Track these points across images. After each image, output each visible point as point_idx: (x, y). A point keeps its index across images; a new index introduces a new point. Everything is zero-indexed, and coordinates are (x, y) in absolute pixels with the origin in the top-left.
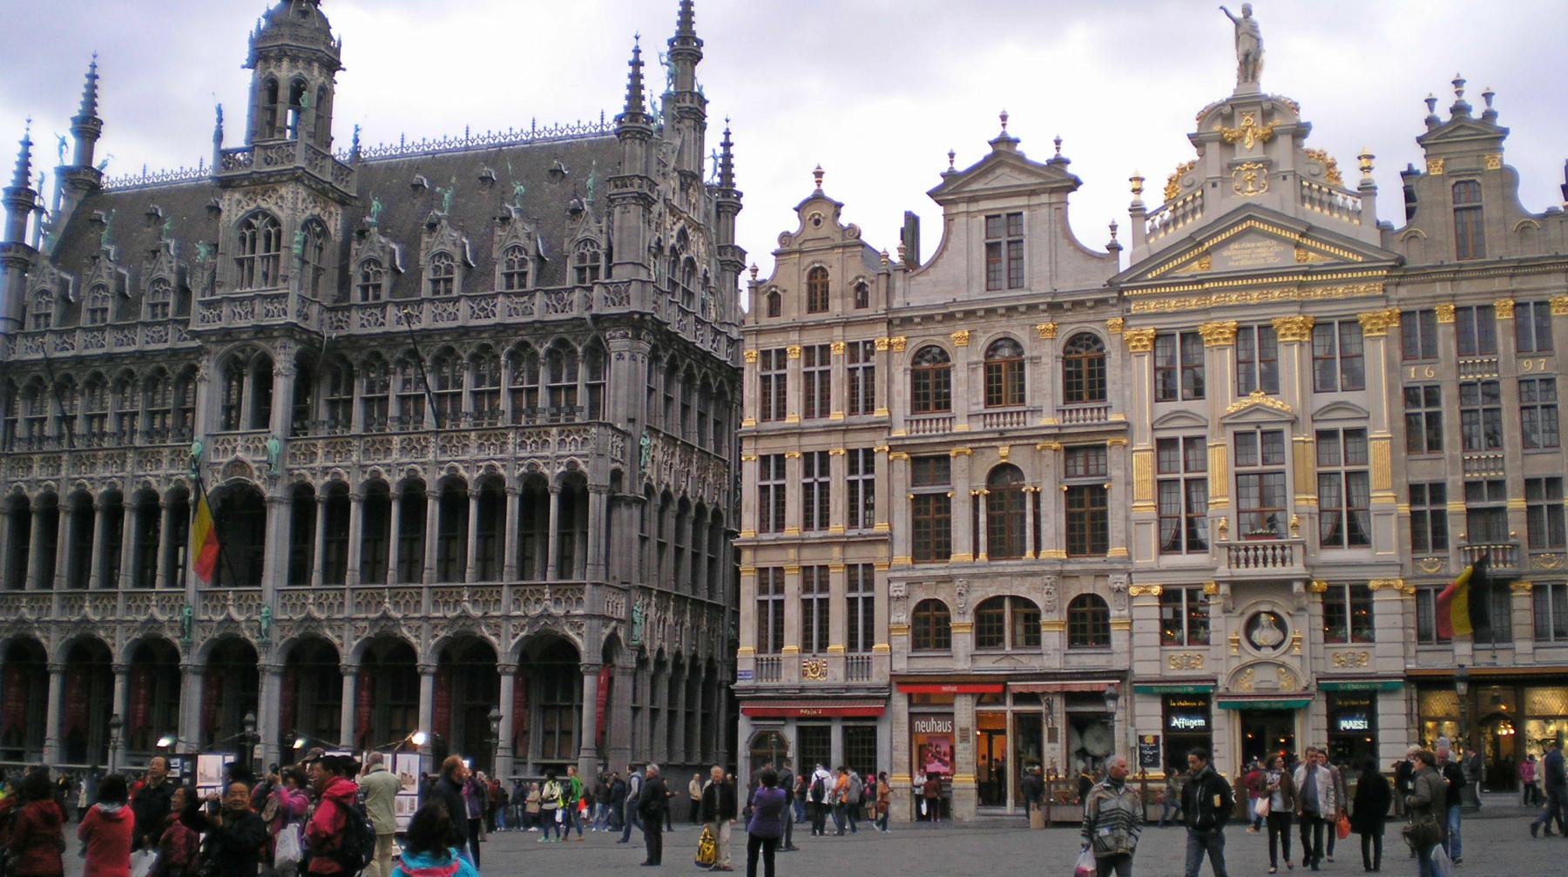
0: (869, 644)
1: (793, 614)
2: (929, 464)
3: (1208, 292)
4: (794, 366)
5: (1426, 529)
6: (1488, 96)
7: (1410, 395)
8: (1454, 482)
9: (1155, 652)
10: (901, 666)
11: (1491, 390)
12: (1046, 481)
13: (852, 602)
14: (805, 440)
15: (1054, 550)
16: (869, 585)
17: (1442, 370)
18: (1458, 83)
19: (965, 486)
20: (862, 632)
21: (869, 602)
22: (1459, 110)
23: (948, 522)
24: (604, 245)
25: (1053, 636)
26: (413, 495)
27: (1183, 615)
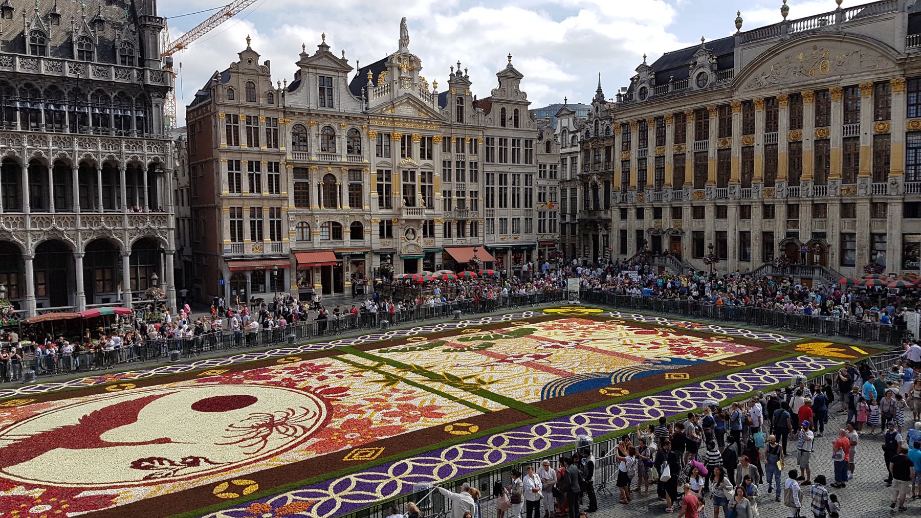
0: (280, 239)
1: (247, 227)
2: (301, 171)
3: (394, 121)
4: (242, 123)
5: (447, 204)
6: (466, 70)
7: (444, 162)
8: (454, 191)
9: (379, 241)
10: (294, 246)
11: (463, 163)
12: (344, 183)
13: (272, 223)
14: (249, 156)
15: (346, 206)
16: (279, 216)
17: (453, 156)
18: (459, 64)
19: (315, 180)
20: (277, 233)
21: (279, 222)
22: (459, 73)
23: (308, 193)
24: (137, 47)
25: (347, 236)
26: (63, 167)
27: (386, 230)
